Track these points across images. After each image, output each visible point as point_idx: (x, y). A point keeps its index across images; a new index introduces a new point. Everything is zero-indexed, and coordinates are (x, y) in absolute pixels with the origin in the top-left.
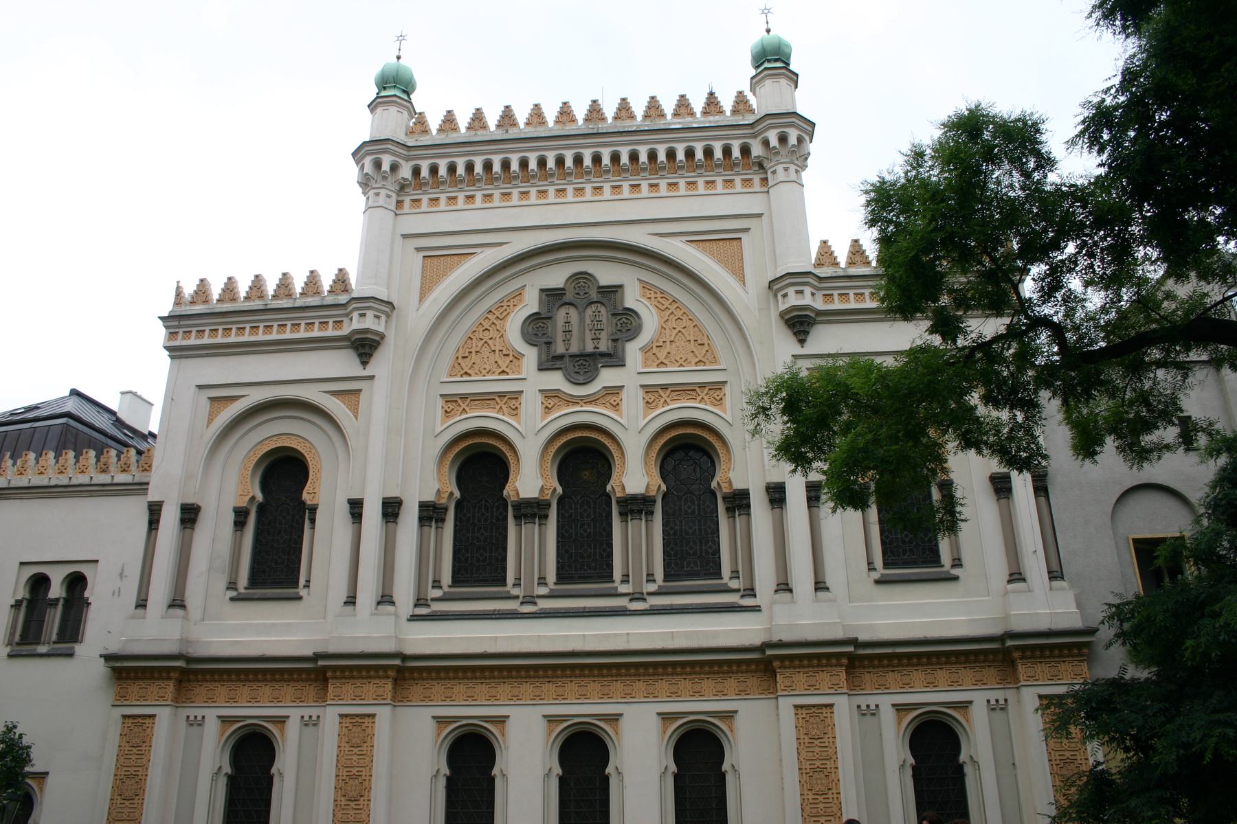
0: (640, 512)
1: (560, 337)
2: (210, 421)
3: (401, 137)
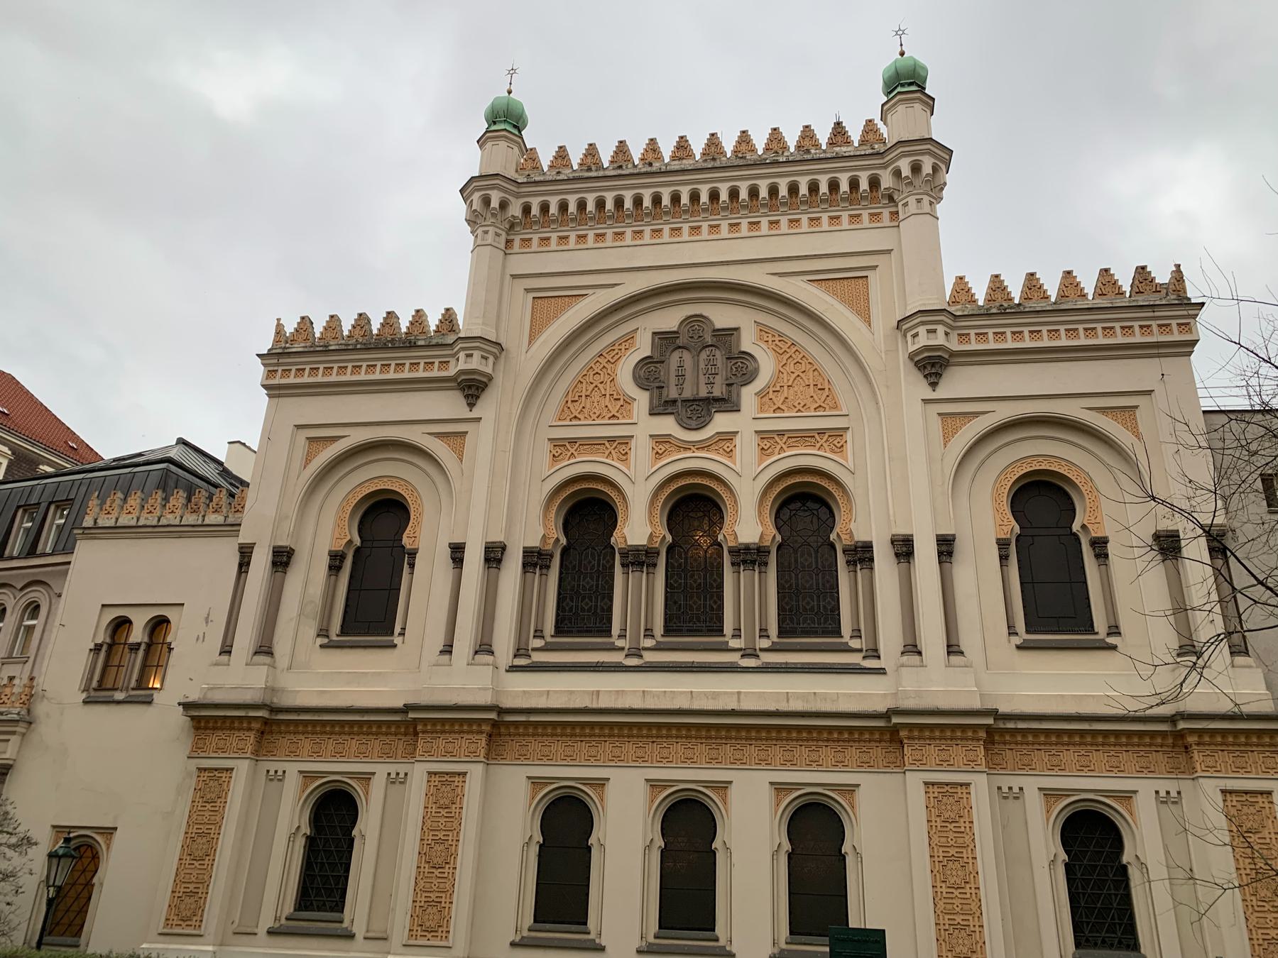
0: (753, 562)
1: (673, 380)
2: (308, 461)
3: (511, 173)
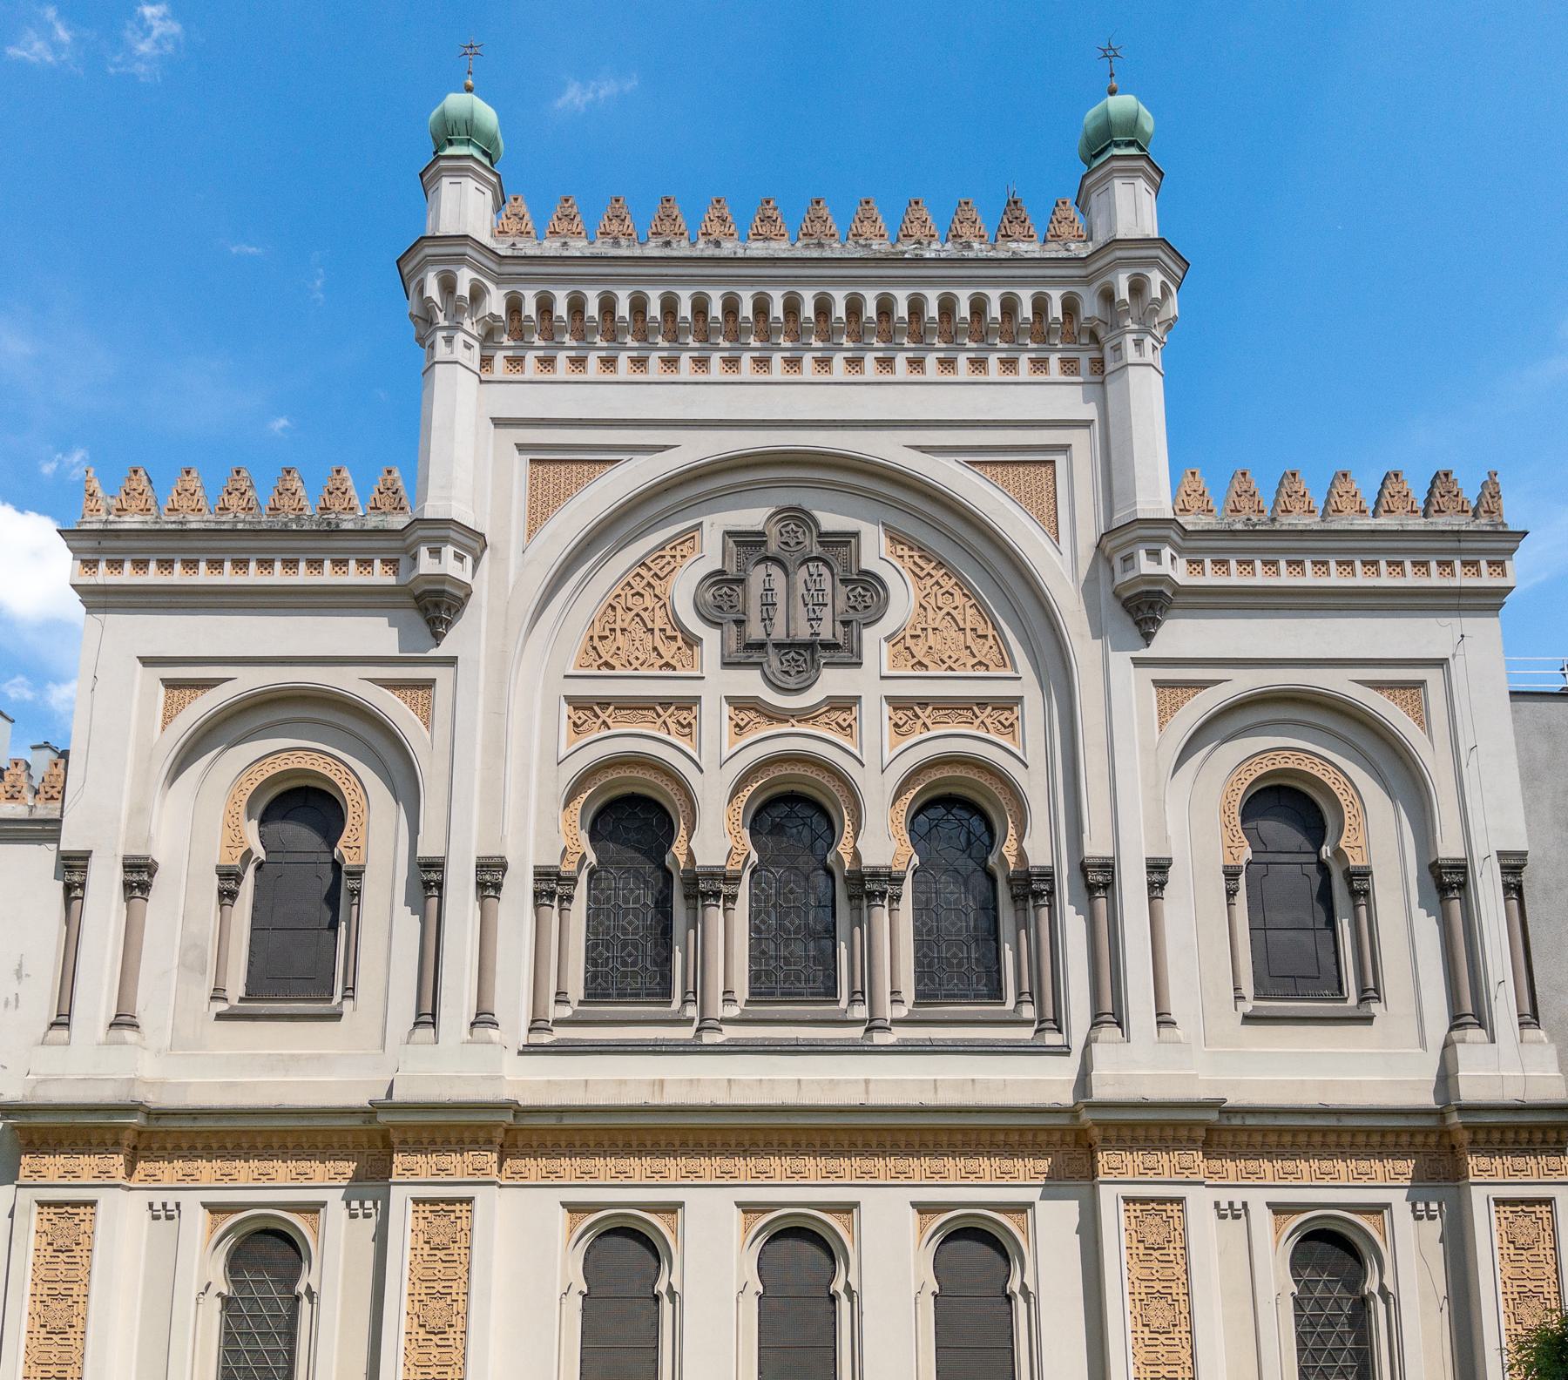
0: (882, 895)
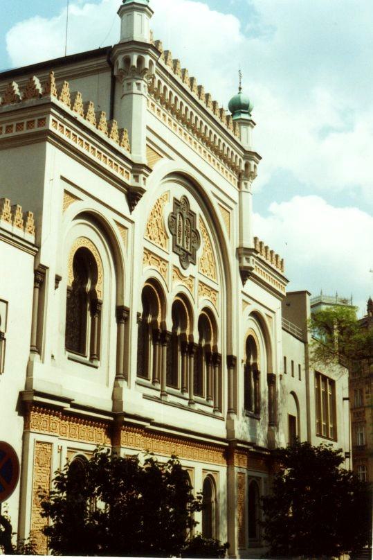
2: (65, 207)
